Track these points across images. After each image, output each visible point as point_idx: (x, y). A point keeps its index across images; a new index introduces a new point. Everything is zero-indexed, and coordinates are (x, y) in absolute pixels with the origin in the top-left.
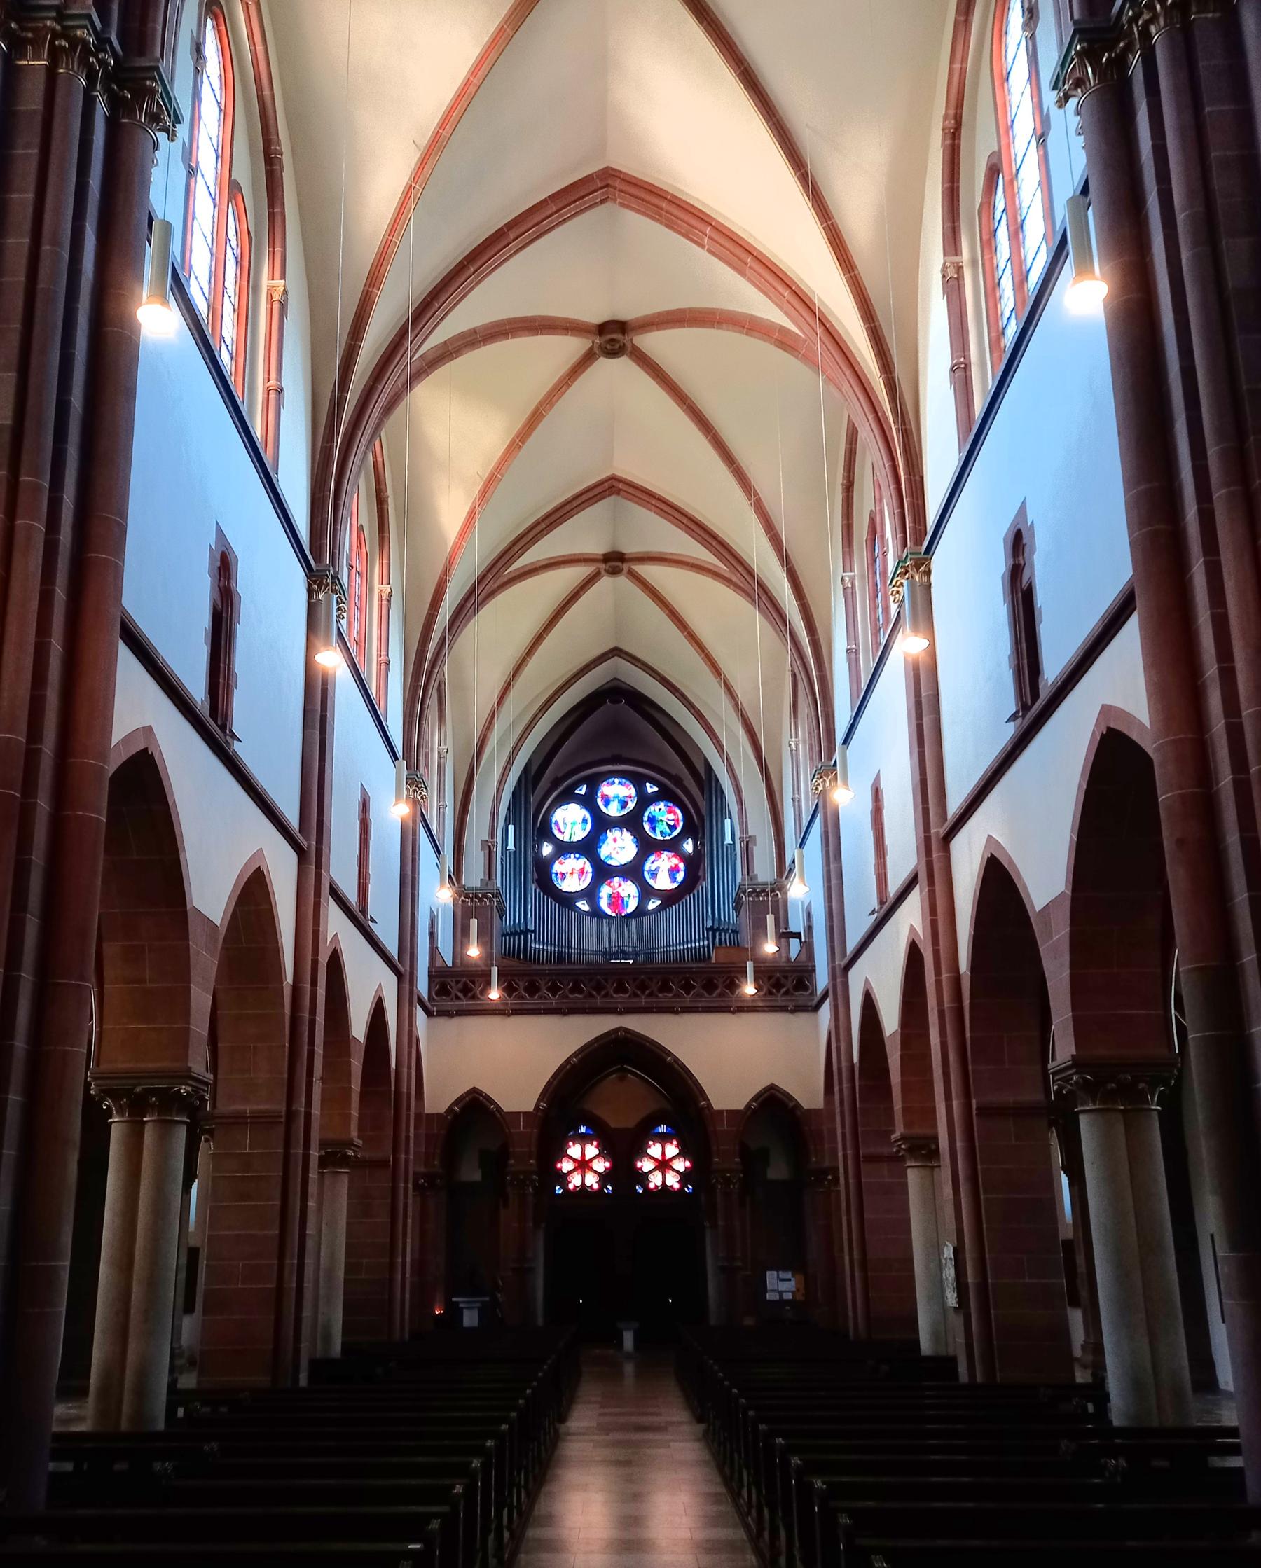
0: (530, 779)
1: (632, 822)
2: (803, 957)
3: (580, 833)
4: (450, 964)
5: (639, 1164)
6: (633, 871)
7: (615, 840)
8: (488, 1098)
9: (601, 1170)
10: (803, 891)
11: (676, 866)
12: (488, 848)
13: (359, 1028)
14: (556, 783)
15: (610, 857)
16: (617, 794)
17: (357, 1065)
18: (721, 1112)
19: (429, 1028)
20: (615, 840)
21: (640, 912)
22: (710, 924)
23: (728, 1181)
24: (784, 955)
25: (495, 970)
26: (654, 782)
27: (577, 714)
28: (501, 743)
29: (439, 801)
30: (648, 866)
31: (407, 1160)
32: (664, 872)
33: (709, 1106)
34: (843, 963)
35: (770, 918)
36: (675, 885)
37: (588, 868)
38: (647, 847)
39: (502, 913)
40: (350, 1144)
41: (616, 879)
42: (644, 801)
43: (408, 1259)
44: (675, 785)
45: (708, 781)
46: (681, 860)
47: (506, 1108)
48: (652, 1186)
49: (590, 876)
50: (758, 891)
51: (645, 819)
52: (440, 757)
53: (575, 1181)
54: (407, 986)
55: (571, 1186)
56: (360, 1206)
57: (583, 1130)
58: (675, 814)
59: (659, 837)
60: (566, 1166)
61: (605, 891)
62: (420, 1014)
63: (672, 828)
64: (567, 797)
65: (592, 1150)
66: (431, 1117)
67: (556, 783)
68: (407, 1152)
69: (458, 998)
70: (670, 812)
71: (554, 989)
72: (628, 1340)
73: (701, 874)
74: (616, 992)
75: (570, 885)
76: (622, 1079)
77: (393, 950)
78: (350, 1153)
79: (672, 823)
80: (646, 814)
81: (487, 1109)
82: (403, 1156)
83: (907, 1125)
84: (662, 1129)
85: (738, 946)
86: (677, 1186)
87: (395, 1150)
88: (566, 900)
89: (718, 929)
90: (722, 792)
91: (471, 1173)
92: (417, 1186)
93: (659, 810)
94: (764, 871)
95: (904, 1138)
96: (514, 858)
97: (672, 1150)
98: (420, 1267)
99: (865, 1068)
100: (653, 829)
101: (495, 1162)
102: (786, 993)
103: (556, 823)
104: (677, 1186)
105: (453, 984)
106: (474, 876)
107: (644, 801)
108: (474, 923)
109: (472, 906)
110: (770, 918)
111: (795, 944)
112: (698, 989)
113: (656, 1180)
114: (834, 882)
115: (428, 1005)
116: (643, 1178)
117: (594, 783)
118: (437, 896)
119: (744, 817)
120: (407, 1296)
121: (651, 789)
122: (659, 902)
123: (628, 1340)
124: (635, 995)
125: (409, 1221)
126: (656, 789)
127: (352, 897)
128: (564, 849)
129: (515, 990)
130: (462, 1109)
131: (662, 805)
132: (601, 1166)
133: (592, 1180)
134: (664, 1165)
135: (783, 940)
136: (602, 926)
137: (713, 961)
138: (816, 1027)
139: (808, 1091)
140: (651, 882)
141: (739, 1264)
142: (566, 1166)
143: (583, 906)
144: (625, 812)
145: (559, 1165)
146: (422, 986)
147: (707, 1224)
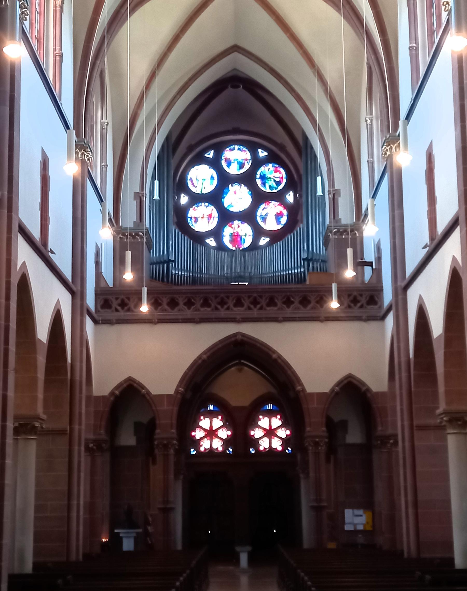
0: (171, 146)
1: (248, 179)
2: (374, 281)
4: (111, 285)
5: (252, 433)
6: (248, 216)
7: (235, 193)
8: (140, 385)
9: (225, 437)
10: (374, 232)
11: (281, 212)
12: (139, 198)
13: (43, 332)
14: (190, 149)
16: (237, 158)
17: (41, 360)
18: (312, 394)
19: (96, 334)
20: (235, 193)
21: (254, 246)
22: (304, 256)
23: (317, 444)
24: (360, 279)
25: (145, 290)
26: (265, 148)
27: (206, 96)
28: (149, 118)
29: (101, 162)
31: (80, 430)
32: (272, 216)
33: (304, 390)
34: (404, 284)
35: (350, 251)
36: (280, 227)
37: (215, 214)
38: (260, 198)
39: (150, 247)
40: (38, 418)
41: (236, 223)
42: (257, 163)
43: (82, 502)
45: (304, 148)
46: (285, 208)
47: (154, 392)
48: (261, 448)
49: (216, 220)
50: (343, 231)
51: (258, 176)
52: (102, 129)
53: (205, 445)
54: (78, 301)
55: (202, 449)
56: (46, 464)
57: (211, 407)
58: (280, 173)
59: (268, 190)
60: (198, 434)
61: (227, 231)
62: (89, 324)
63: (278, 183)
64: (199, 159)
65: (217, 423)
66: (98, 398)
67: (190, 149)
68: (80, 424)
69: (117, 310)
70: (276, 171)
71: (189, 304)
72: (244, 558)
73: (299, 218)
74: (235, 305)
76: (240, 370)
77: (67, 273)
78: (37, 424)
79: (278, 180)
80: (259, 173)
81: (140, 392)
82: (76, 427)
83: (448, 403)
84: (270, 407)
85: (324, 271)
86: (280, 448)
87: (71, 422)
88: (198, 238)
89: (311, 259)
90: (315, 157)
91: (128, 439)
92: (87, 449)
93: (268, 170)
94: (346, 216)
95: (445, 413)
96: (158, 206)
97: (276, 422)
98: (91, 508)
99: (418, 360)
100: (264, 184)
101: (146, 431)
102: (362, 307)
103: (191, 180)
104: (280, 448)
105: (114, 300)
106: (129, 219)
107: (257, 163)
108: (129, 254)
109: (126, 241)
110: (350, 251)
111: (368, 271)
112: (296, 304)
113: (264, 444)
114: (397, 224)
115: (95, 316)
116: (255, 442)
117: (219, 149)
118: (101, 235)
119: (331, 175)
120: (81, 529)
121: (262, 154)
122: (268, 240)
123: (244, 558)
124: (249, 308)
125: (82, 474)
126: (266, 154)
127: (36, 233)
128: (196, 199)
129: (160, 304)
130: (121, 393)
131: (270, 165)
132: (224, 434)
133: (217, 445)
134: (270, 433)
135: (359, 268)
136: (225, 255)
137: (308, 282)
138: (383, 331)
139: (376, 380)
140: (262, 224)
141: (325, 504)
142: (198, 434)
143: (211, 242)
145: (193, 434)
146: (90, 300)
147: (302, 476)
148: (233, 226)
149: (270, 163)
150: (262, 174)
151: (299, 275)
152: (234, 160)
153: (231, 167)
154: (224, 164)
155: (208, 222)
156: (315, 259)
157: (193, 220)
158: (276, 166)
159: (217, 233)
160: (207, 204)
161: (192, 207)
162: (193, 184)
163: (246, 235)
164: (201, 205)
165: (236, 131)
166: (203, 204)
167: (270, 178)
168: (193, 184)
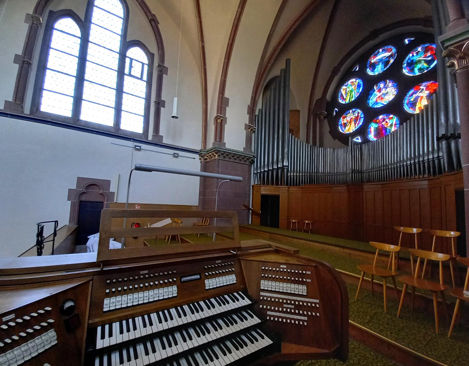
1: (392, 73)
3: (355, 95)
7: (380, 90)
15: (376, 103)
20: (380, 90)
41: (381, 117)
44: (425, 26)
49: (362, 120)
58: (431, 49)
63: (429, 63)
75: (351, 128)
79: (430, 58)
88: (345, 139)
100: (412, 70)
131: (419, 49)
144: (388, 67)
148: (377, 121)
149: (418, 45)
150: (409, 61)
151: (436, 161)
152: (379, 62)
153: (376, 70)
155: (355, 124)
159: (363, 131)
160: (354, 110)
161: (341, 116)
163: (391, 125)
164: (349, 113)
166: (351, 111)
167: (419, 61)
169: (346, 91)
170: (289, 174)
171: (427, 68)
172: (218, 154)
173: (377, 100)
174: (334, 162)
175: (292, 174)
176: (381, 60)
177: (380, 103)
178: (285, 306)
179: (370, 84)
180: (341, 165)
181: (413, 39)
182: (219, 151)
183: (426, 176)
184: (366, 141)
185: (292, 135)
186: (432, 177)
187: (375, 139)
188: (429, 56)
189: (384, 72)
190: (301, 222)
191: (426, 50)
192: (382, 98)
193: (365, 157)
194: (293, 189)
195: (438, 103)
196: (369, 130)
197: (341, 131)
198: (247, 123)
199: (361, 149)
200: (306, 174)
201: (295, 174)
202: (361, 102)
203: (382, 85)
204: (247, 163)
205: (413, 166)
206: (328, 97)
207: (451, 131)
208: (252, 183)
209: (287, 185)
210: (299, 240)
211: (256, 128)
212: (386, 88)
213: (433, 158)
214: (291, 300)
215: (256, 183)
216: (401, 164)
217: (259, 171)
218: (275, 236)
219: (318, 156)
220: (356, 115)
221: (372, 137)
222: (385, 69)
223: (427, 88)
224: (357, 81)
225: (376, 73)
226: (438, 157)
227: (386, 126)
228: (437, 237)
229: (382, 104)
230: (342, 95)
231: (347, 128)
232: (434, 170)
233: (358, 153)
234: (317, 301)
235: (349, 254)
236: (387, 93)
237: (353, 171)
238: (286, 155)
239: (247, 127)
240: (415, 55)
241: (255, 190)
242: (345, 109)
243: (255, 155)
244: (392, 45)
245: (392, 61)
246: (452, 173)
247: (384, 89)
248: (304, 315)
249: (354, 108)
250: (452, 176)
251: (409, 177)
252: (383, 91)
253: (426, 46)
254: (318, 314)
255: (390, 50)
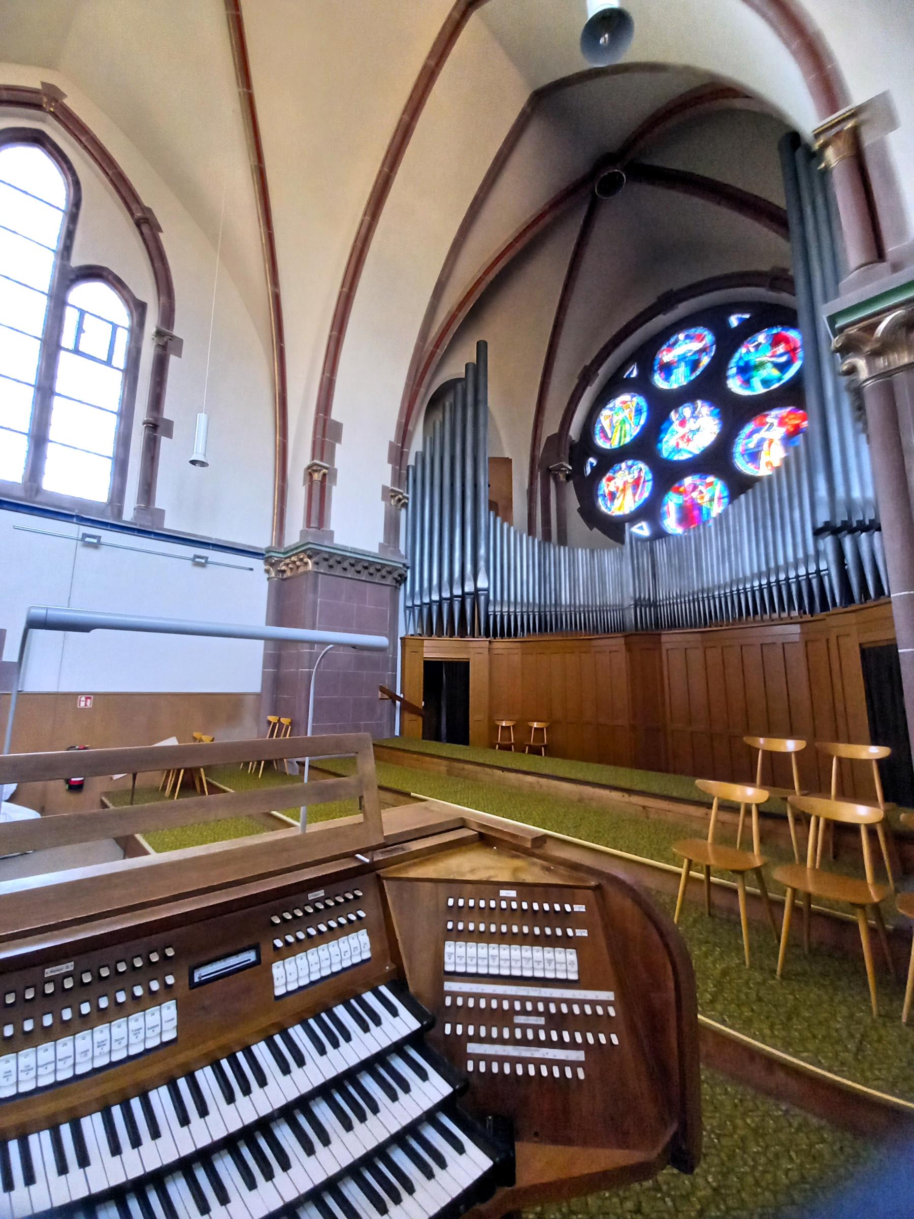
1: (708, 386)
6: (716, 460)
15: (677, 448)
20: (683, 423)
30: (742, 443)
38: (737, 414)
41: (688, 481)
44: (772, 287)
49: (649, 485)
51: (733, 371)
58: (786, 340)
61: (672, 502)
79: (783, 359)
100: (747, 383)
131: (761, 338)
144: (698, 373)
148: (682, 489)
149: (758, 330)
151: (815, 582)
152: (679, 360)
153: (673, 378)
154: (659, 381)
155: (634, 494)
156: (860, 523)
157: (607, 498)
158: (775, 331)
160: (630, 463)
161: (604, 475)
162: (606, 438)
163: (712, 500)
164: (621, 469)
165: (667, 302)
166: (623, 465)
167: (762, 365)
168: (606, 438)
169: (611, 421)
170: (491, 609)
171: (780, 380)
172: (314, 559)
173: (678, 444)
174: (593, 582)
175: (498, 609)
176: (683, 358)
177: (686, 451)
178: (519, 1019)
179: (661, 408)
180: (610, 587)
181: (747, 316)
182: (317, 552)
183: (795, 613)
184: (659, 534)
185: (496, 515)
186: (808, 617)
187: (679, 531)
188: (781, 355)
189: (691, 383)
190: (521, 726)
191: (776, 341)
192: (689, 440)
193: (662, 570)
194: (501, 645)
195: (813, 453)
196: (665, 508)
197: (603, 508)
198: (388, 484)
199: (652, 552)
200: (530, 610)
201: (505, 609)
202: (644, 447)
203: (686, 410)
204: (389, 581)
205: (765, 591)
206: (574, 432)
207: (842, 517)
208: (402, 633)
209: (487, 635)
210: (520, 776)
211: (410, 496)
212: (696, 418)
213: (808, 574)
214: (535, 1000)
215: (411, 632)
216: (741, 587)
217: (418, 602)
218: (461, 765)
219: (557, 565)
220: (636, 475)
221: (671, 524)
222: (693, 377)
223: (782, 422)
224: (634, 399)
225: (675, 386)
226: (818, 571)
227: (699, 501)
228: (840, 760)
229: (690, 453)
230: (603, 430)
231: (617, 502)
232: (812, 600)
233: (646, 560)
234: (609, 996)
235: (644, 807)
236: (698, 430)
237: (638, 603)
238: (482, 564)
239: (388, 494)
240: (752, 350)
241: (408, 650)
242: (610, 460)
243: (409, 563)
244: (705, 326)
245: (705, 360)
246: (849, 609)
247: (692, 420)
248: (573, 1045)
249: (630, 459)
250: (853, 614)
251: (758, 617)
252: (691, 425)
253: (775, 331)
254: (615, 1040)
255: (700, 338)
